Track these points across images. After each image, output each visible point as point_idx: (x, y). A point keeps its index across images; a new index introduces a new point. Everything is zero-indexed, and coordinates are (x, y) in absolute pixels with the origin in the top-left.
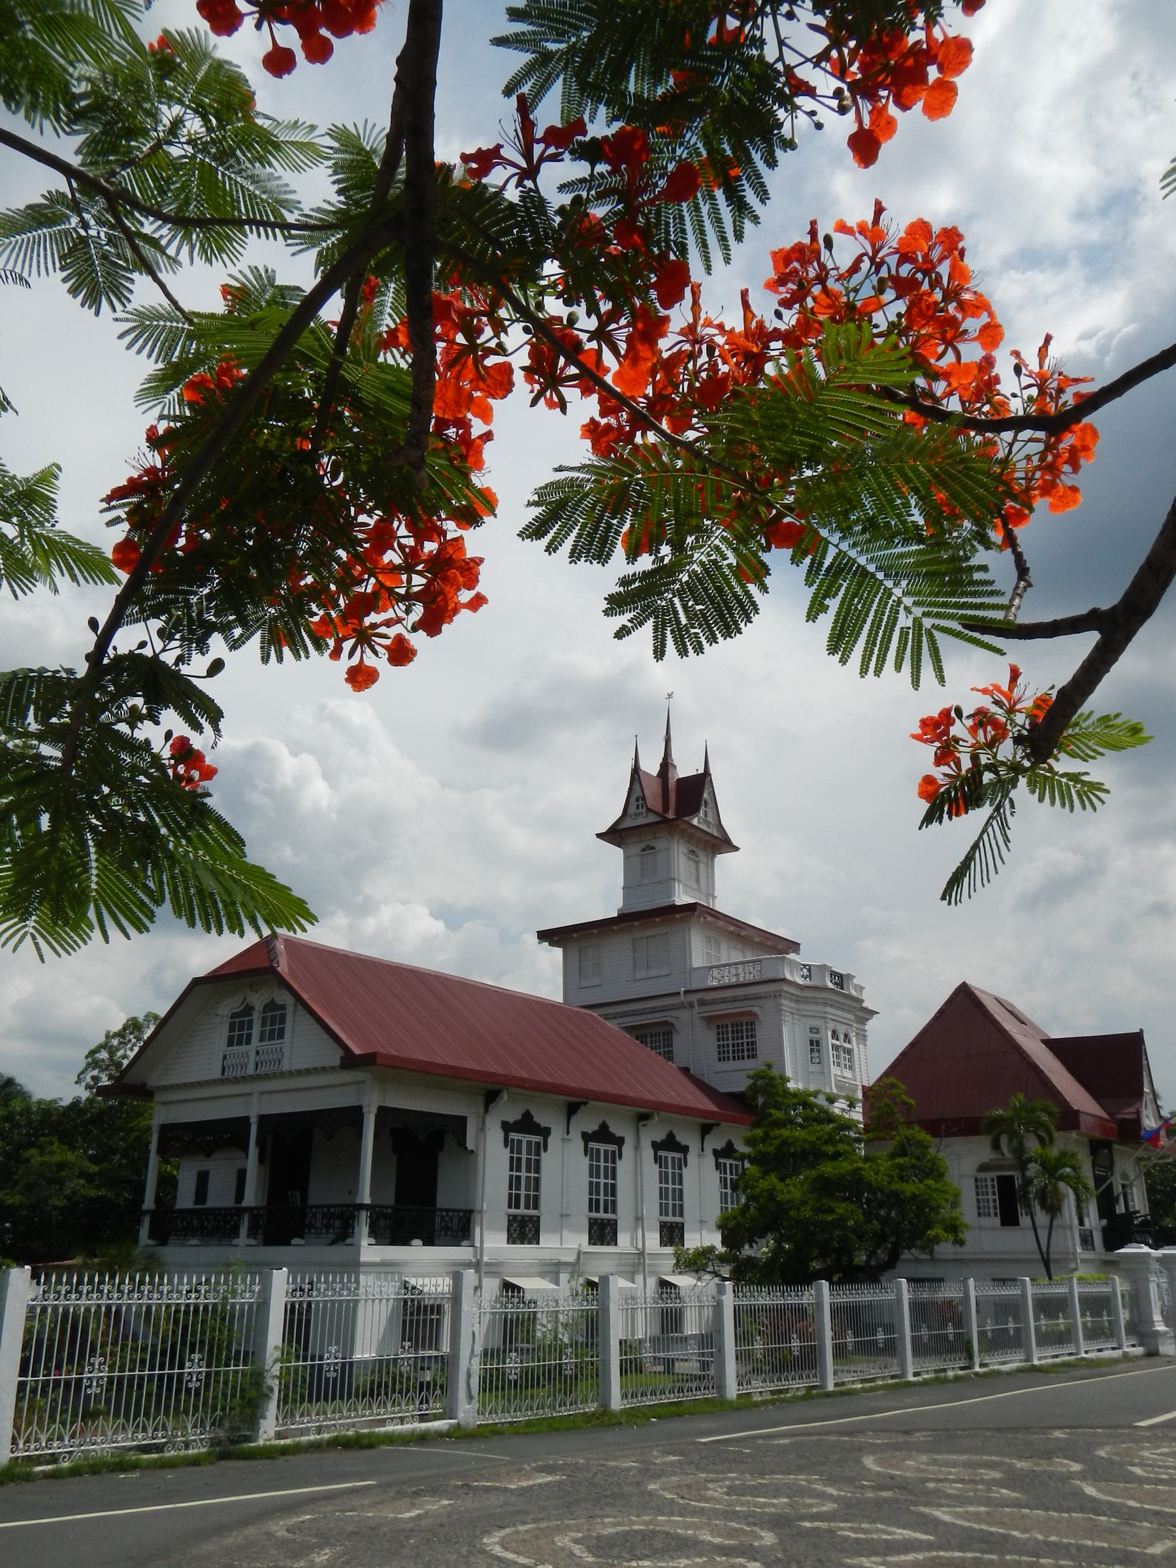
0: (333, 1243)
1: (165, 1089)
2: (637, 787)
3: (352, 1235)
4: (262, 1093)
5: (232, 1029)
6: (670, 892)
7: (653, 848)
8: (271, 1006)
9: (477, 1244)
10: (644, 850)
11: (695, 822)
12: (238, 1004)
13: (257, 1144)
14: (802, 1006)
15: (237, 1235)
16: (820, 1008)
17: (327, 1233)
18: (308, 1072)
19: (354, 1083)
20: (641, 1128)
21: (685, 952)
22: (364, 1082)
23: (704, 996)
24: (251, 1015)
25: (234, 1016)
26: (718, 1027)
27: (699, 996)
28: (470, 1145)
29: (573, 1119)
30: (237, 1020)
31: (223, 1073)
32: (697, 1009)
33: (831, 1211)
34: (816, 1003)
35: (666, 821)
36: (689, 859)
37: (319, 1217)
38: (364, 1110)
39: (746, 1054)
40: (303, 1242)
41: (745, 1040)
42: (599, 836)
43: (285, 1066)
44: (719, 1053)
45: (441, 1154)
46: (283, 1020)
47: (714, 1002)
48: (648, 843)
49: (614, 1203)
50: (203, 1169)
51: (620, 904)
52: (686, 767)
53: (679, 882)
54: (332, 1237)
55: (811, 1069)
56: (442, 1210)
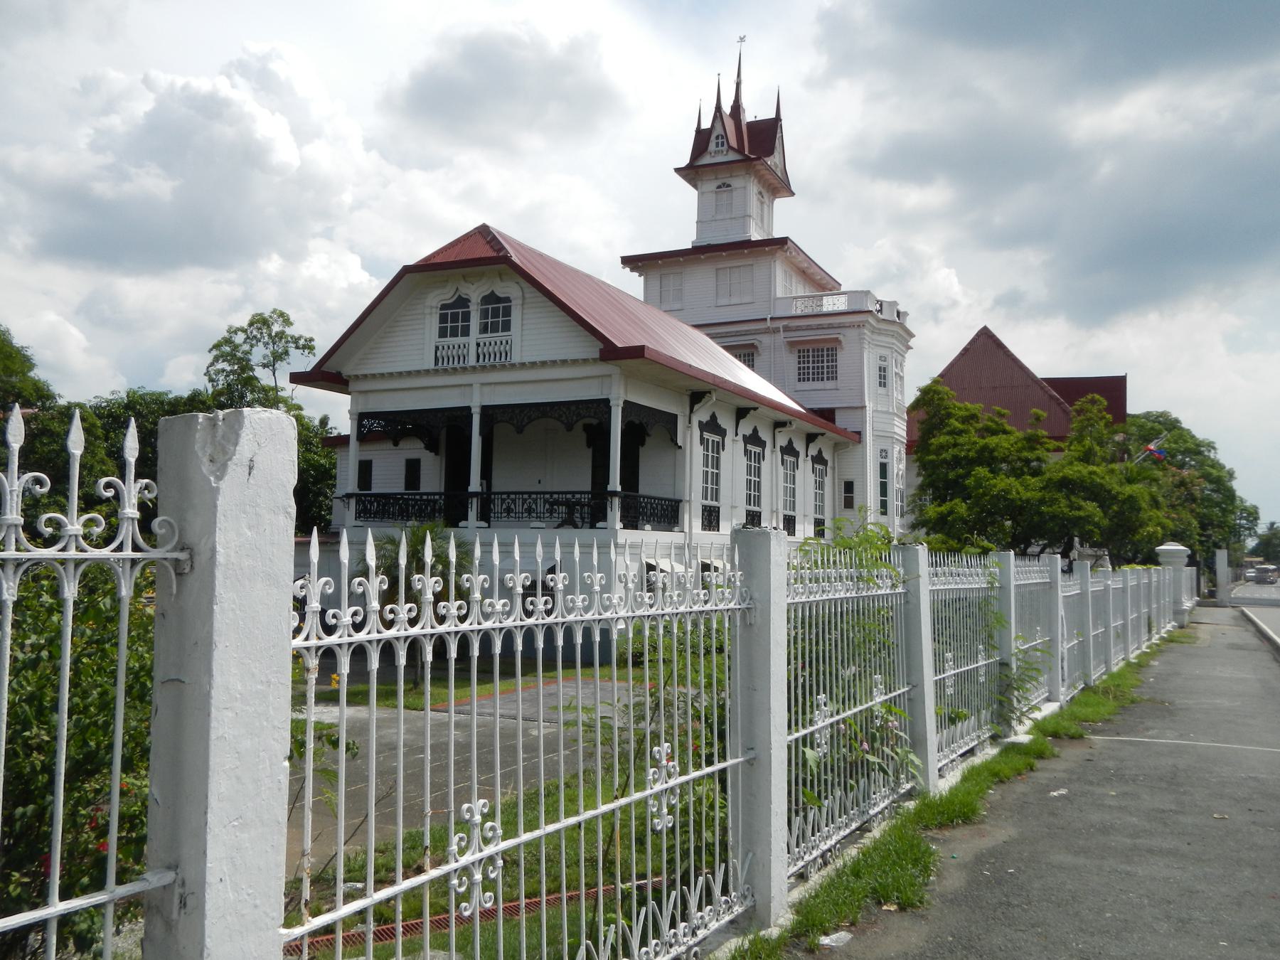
0: (559, 527)
1: (357, 377)
3: (604, 518)
4: (483, 384)
5: (443, 319)
6: (745, 228)
7: (729, 186)
8: (491, 298)
9: (687, 530)
11: (769, 163)
13: (481, 433)
14: (875, 337)
18: (544, 364)
19: (599, 376)
22: (610, 376)
23: (789, 322)
25: (444, 307)
26: (799, 351)
27: (785, 323)
28: (680, 443)
29: (742, 422)
30: (449, 312)
31: (436, 363)
33: (1079, 508)
34: (887, 335)
35: (747, 159)
36: (758, 199)
38: (611, 403)
39: (825, 376)
40: (543, 525)
41: (825, 364)
42: (678, 170)
43: (516, 358)
44: (799, 374)
46: (507, 312)
47: (798, 329)
49: (759, 497)
50: (363, 458)
51: (694, 238)
52: (755, 111)
53: (754, 219)
55: (879, 392)
56: (644, 497)
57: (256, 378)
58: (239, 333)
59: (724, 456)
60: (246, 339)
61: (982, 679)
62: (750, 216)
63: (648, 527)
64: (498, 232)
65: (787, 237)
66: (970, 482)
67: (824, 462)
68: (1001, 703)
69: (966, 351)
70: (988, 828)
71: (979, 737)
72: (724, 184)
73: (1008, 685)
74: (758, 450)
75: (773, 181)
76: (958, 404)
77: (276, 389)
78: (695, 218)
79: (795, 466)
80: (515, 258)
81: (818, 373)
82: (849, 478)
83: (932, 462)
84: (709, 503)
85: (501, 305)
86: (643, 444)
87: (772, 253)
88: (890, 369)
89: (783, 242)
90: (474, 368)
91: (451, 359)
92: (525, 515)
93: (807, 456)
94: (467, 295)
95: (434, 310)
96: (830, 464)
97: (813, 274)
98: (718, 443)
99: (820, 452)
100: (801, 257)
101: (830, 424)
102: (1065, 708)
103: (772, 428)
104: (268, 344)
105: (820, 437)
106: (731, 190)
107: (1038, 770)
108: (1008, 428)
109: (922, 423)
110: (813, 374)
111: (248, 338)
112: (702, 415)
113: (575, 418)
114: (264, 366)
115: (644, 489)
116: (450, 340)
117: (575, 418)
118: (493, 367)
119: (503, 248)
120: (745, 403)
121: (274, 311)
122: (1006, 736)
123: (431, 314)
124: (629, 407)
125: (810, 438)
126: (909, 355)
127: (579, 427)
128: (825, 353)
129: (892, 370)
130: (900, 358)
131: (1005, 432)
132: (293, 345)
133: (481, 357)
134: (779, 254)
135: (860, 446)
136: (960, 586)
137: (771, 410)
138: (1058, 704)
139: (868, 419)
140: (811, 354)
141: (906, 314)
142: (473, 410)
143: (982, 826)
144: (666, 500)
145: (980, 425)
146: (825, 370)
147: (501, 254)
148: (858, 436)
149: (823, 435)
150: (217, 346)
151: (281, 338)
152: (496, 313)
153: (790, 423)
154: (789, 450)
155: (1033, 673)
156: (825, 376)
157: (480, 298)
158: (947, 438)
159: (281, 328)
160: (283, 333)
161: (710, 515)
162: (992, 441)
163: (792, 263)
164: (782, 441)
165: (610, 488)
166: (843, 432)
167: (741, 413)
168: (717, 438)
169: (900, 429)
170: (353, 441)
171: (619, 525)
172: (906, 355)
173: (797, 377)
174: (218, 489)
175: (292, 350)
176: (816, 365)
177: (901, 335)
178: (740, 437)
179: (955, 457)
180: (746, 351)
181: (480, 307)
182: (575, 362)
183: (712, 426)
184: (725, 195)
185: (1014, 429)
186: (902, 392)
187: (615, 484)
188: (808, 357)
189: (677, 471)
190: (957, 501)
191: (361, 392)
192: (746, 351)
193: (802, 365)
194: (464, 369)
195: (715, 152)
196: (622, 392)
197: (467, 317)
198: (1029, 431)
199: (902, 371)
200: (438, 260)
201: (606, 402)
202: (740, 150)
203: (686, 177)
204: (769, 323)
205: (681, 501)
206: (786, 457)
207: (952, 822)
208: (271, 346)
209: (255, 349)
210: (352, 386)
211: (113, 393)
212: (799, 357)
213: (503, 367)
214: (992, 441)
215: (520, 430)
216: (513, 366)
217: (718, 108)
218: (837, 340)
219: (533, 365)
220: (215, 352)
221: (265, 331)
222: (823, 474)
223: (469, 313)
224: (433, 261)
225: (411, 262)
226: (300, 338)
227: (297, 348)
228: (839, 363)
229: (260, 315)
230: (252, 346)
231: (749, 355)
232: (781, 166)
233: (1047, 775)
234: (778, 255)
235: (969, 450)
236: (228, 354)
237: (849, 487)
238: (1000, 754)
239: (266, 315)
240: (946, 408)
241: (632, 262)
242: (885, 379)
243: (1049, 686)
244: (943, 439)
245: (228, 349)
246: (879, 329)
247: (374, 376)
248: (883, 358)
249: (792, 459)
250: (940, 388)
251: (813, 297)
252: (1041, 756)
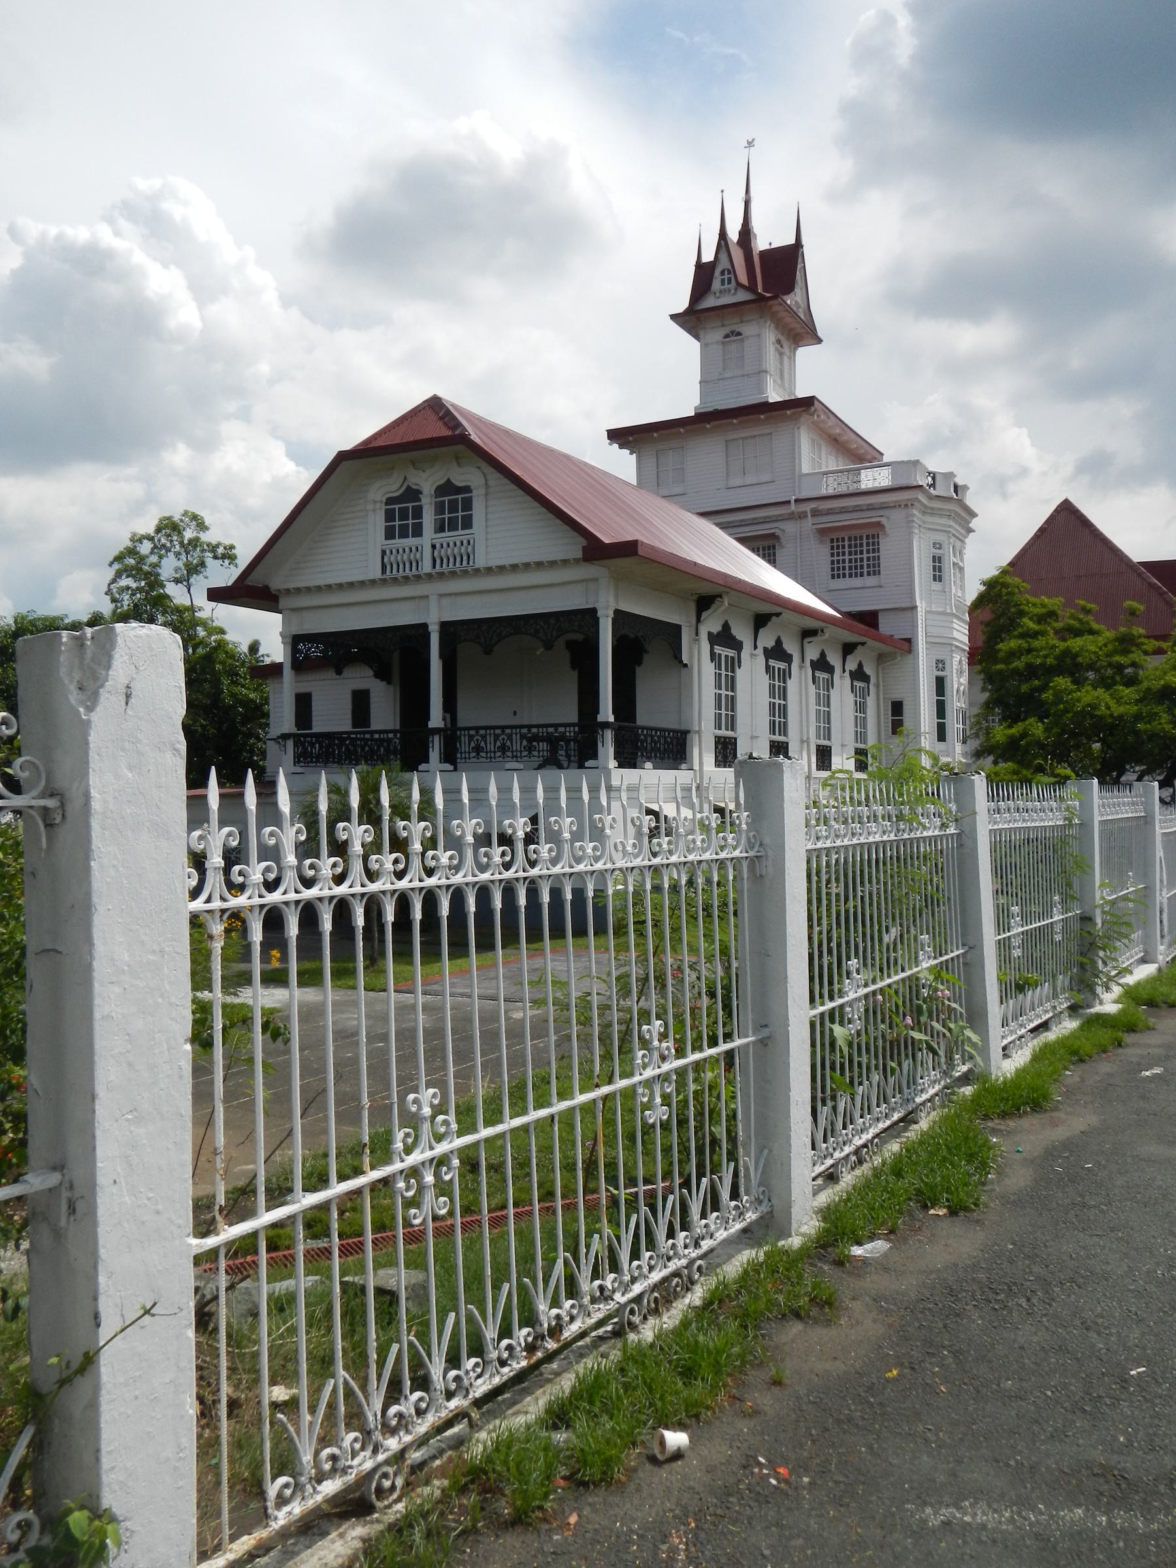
0: (540, 767)
1: (288, 591)
2: (723, 257)
3: (595, 756)
4: (441, 595)
5: (389, 516)
6: (761, 387)
7: (739, 334)
8: (446, 489)
9: (696, 767)
10: (727, 336)
12: (395, 487)
13: (441, 656)
14: (928, 519)
16: (944, 521)
17: (530, 755)
19: (582, 581)
20: (807, 646)
21: (793, 455)
22: (596, 580)
25: (390, 501)
26: (832, 540)
27: (814, 505)
28: (685, 660)
30: (397, 507)
31: (384, 571)
32: (810, 520)
34: (941, 516)
35: (761, 299)
36: (776, 349)
37: (489, 739)
38: (599, 614)
39: (865, 570)
40: (521, 766)
41: (865, 556)
42: (674, 317)
43: (480, 562)
44: (833, 569)
45: (639, 671)
46: (468, 505)
47: (830, 512)
48: (733, 328)
50: (302, 690)
51: (697, 402)
54: (537, 761)
56: (643, 728)
57: (167, 597)
58: (145, 541)
59: (740, 674)
60: (153, 549)
61: (1058, 938)
62: (766, 372)
63: (649, 765)
64: (452, 405)
65: (813, 398)
66: (1047, 696)
67: (865, 678)
68: (1082, 966)
69: (1042, 531)
70: (1062, 1115)
71: (1055, 1007)
72: (732, 332)
73: (1091, 944)
74: (783, 665)
75: (794, 325)
76: (1032, 599)
77: (192, 609)
78: (697, 377)
79: (830, 684)
80: (474, 437)
81: (856, 568)
82: (897, 697)
83: (1000, 672)
84: (723, 732)
85: (460, 497)
86: (640, 663)
87: (795, 418)
88: (947, 557)
89: (808, 403)
90: (429, 576)
91: (401, 566)
92: (499, 754)
93: (844, 671)
95: (378, 506)
96: (873, 680)
97: (847, 441)
98: (733, 658)
99: (860, 666)
100: (831, 422)
101: (873, 630)
102: (1165, 970)
103: (800, 638)
104: (179, 553)
105: (859, 647)
106: (742, 340)
107: (1128, 1045)
108: (1095, 626)
109: (987, 625)
110: (850, 568)
111: (155, 547)
112: (712, 624)
113: (555, 634)
114: (177, 581)
115: (644, 718)
117: (555, 634)
118: (453, 574)
119: (459, 424)
120: (765, 608)
121: (185, 514)
122: (1089, 1006)
123: (374, 510)
124: (620, 617)
125: (848, 649)
126: (970, 540)
127: (560, 644)
128: (865, 541)
129: (950, 559)
130: (958, 544)
131: (1092, 632)
132: (211, 555)
133: (438, 561)
134: (805, 418)
135: (911, 656)
136: (1029, 824)
137: (799, 616)
138: (1156, 965)
139: (920, 622)
140: (846, 543)
141: (965, 488)
142: (431, 628)
143: (1056, 1114)
144: (669, 731)
145: (1059, 625)
146: (865, 563)
147: (457, 432)
148: (907, 645)
149: (863, 644)
150: (119, 558)
151: (195, 547)
152: (453, 507)
153: (822, 631)
154: (821, 664)
155: (1124, 930)
156: (865, 570)
158: (1020, 642)
159: (195, 534)
160: (197, 539)
161: (725, 748)
162: (1075, 644)
163: (821, 429)
164: (812, 654)
165: (600, 718)
166: (888, 640)
167: (760, 621)
168: (731, 653)
169: (960, 633)
170: (287, 671)
171: (613, 763)
172: (967, 541)
173: (830, 573)
174: (89, 722)
175: (209, 561)
176: (853, 557)
177: (959, 515)
178: (760, 651)
179: (1029, 666)
180: (766, 543)
181: (434, 500)
182: (552, 564)
183: (724, 638)
184: (734, 346)
185: (1103, 627)
186: (962, 588)
187: (607, 713)
188: (843, 547)
189: (683, 695)
190: (1032, 720)
191: (294, 610)
192: (766, 543)
193: (835, 558)
194: (418, 577)
195: (721, 292)
196: (612, 599)
197: (418, 513)
198: (1122, 629)
199: (962, 560)
200: (380, 443)
201: (593, 611)
202: (752, 288)
203: (682, 326)
204: (793, 507)
205: (689, 732)
206: (818, 674)
207: (1019, 1110)
208: (183, 557)
209: (164, 561)
210: (283, 603)
212: (832, 548)
213: (465, 573)
214: (1075, 644)
215: (488, 651)
216: (477, 571)
217: (723, 234)
218: (879, 525)
219: (502, 569)
220: (116, 566)
221: (175, 538)
222: (865, 693)
223: (420, 508)
224: (374, 444)
225: (348, 446)
226: (217, 546)
227: (215, 557)
228: (882, 553)
229: (169, 518)
230: (161, 557)
231: (769, 548)
232: (803, 305)
233: (1138, 1051)
234: (802, 419)
235: (1046, 657)
236: (132, 568)
237: (897, 708)
238: (1081, 1028)
239: (176, 518)
240: (1017, 605)
241: (619, 436)
242: (940, 571)
243: (1145, 943)
244: (1013, 644)
245: (132, 561)
246: (932, 509)
247: (308, 590)
248: (937, 545)
249: (826, 676)
250: (1009, 580)
251: (848, 471)
252: (1131, 1029)
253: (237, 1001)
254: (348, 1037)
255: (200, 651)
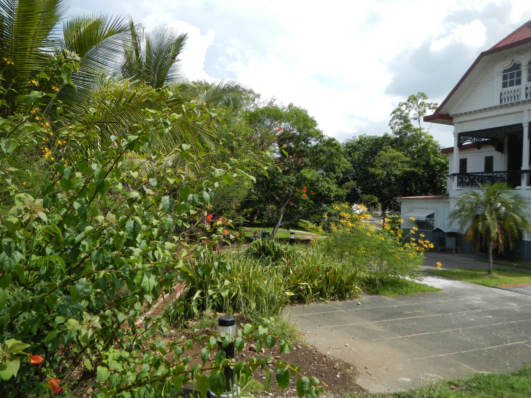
1: (457, 115)
5: (505, 78)
12: (509, 63)
15: (519, 184)
24: (520, 68)
25: (505, 71)
57: (411, 125)
60: (406, 108)
94: (519, 62)
95: (499, 74)
104: (416, 109)
111: (407, 107)
114: (415, 119)
116: (509, 89)
150: (394, 112)
151: (422, 105)
157: (528, 61)
159: (422, 101)
160: (423, 102)
170: (456, 150)
191: (459, 123)
197: (519, 74)
210: (455, 120)
211: (353, 137)
220: (393, 115)
225: (487, 49)
226: (431, 104)
227: (430, 109)
230: (409, 111)
236: (399, 115)
239: (416, 95)
247: (466, 114)
253: (423, 283)
254: (473, 309)
255: (422, 144)
